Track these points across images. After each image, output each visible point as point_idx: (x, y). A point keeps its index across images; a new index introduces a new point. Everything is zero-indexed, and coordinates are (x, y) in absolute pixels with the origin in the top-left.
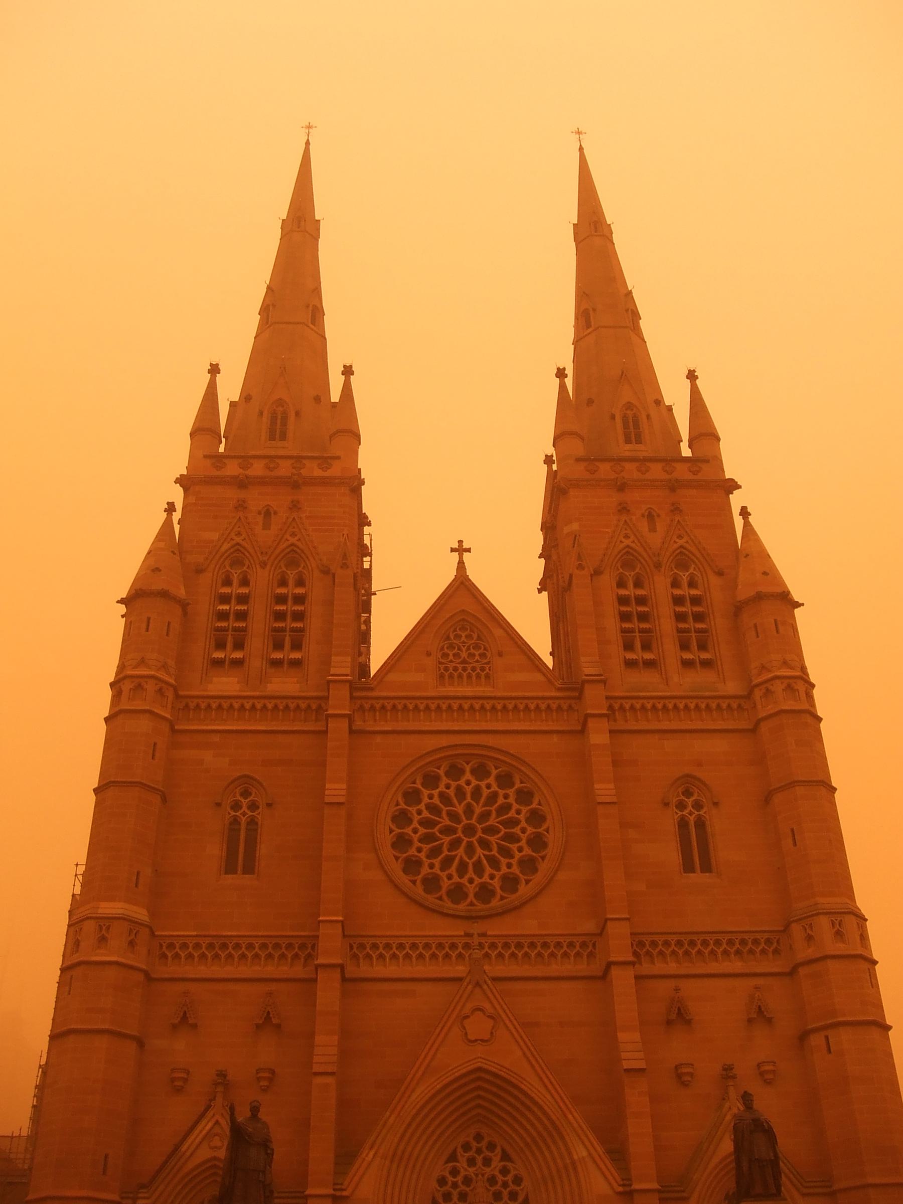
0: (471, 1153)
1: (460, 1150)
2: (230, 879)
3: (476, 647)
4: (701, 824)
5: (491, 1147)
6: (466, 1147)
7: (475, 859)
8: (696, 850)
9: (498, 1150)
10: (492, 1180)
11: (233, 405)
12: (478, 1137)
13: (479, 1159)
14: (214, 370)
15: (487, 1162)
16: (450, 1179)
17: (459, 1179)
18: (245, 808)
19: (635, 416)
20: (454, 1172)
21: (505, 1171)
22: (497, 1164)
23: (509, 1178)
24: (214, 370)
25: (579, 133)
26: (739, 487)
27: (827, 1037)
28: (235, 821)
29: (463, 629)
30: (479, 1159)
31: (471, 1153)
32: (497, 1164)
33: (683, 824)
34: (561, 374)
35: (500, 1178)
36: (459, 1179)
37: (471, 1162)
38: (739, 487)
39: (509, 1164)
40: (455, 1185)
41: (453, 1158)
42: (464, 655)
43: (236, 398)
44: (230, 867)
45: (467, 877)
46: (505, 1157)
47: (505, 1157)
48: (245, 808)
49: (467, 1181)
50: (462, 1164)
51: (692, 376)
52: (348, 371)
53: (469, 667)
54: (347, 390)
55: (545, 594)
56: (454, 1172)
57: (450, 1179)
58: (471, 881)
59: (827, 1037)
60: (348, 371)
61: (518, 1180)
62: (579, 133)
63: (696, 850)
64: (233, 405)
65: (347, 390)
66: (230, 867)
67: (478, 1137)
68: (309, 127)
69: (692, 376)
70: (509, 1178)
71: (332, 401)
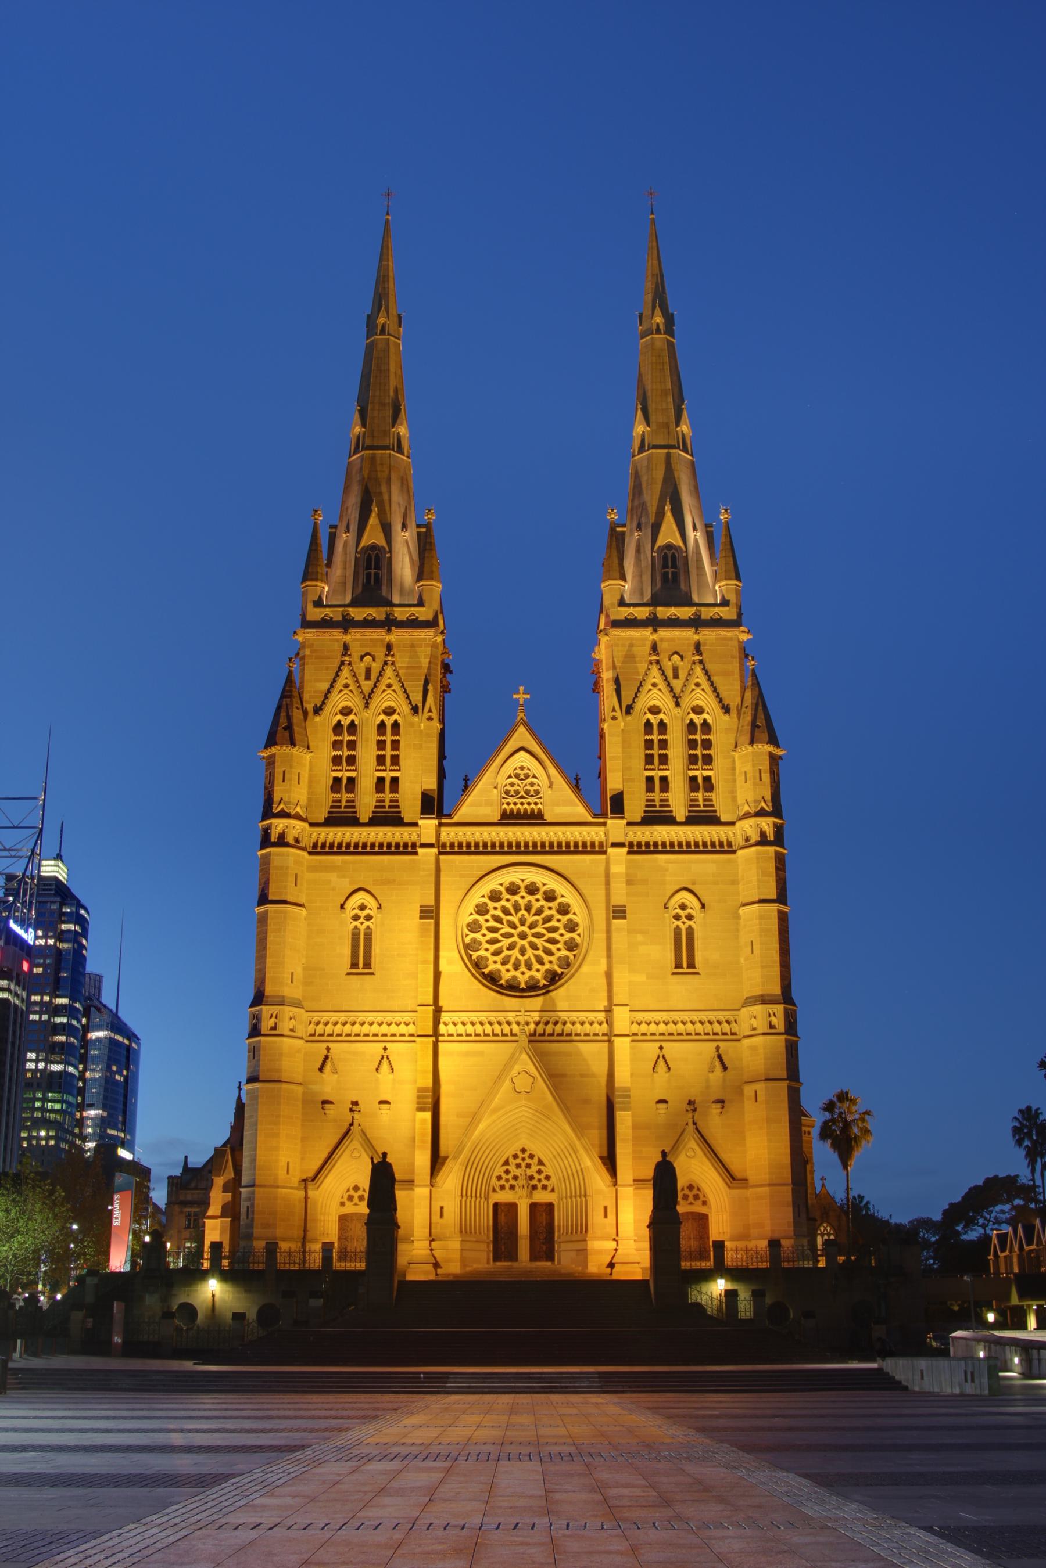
1: (511, 1160)
4: (690, 932)
5: (531, 1156)
6: (515, 1156)
9: (536, 1160)
10: (532, 1178)
12: (523, 1150)
13: (523, 1164)
15: (528, 1166)
16: (504, 1176)
17: (510, 1176)
19: (673, 555)
20: (507, 1172)
21: (539, 1172)
22: (535, 1168)
23: (542, 1176)
30: (523, 1164)
31: (518, 1161)
32: (535, 1168)
33: (677, 932)
35: (536, 1176)
36: (510, 1176)
37: (518, 1166)
39: (542, 1168)
40: (507, 1180)
41: (507, 1163)
47: (540, 1162)
49: (515, 1178)
50: (512, 1168)
56: (507, 1172)
57: (504, 1176)
61: (548, 1178)
67: (523, 1150)
70: (542, 1176)
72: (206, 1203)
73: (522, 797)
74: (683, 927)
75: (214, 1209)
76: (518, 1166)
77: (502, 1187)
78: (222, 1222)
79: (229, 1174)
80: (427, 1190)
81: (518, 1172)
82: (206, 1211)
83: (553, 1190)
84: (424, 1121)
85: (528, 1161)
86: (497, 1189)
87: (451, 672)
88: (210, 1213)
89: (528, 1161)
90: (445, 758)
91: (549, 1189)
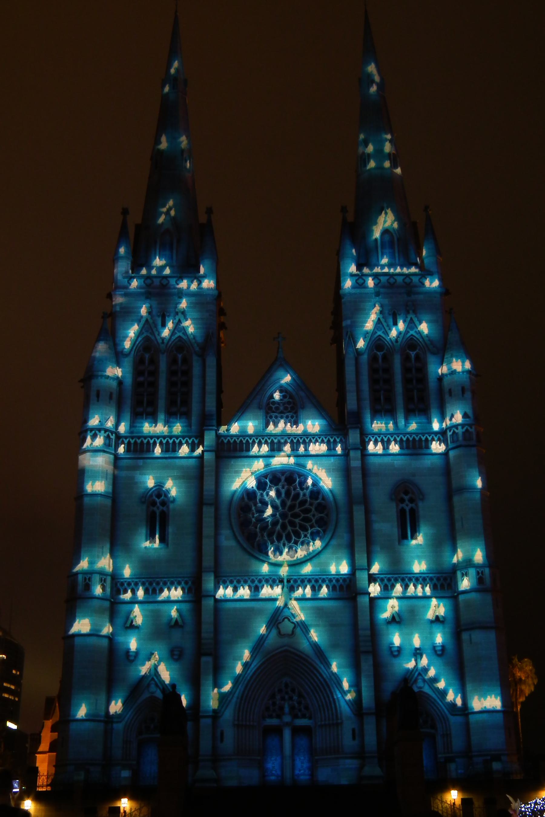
7: (287, 532)
14: (125, 212)
24: (125, 212)
27: (470, 636)
28: (154, 513)
34: (344, 210)
45: (282, 542)
46: (300, 695)
47: (300, 695)
52: (209, 211)
56: (274, 704)
59: (470, 636)
60: (209, 211)
72: (37, 741)
75: (44, 746)
78: (49, 756)
79: (56, 717)
82: (38, 748)
88: (41, 749)
90: (222, 392)
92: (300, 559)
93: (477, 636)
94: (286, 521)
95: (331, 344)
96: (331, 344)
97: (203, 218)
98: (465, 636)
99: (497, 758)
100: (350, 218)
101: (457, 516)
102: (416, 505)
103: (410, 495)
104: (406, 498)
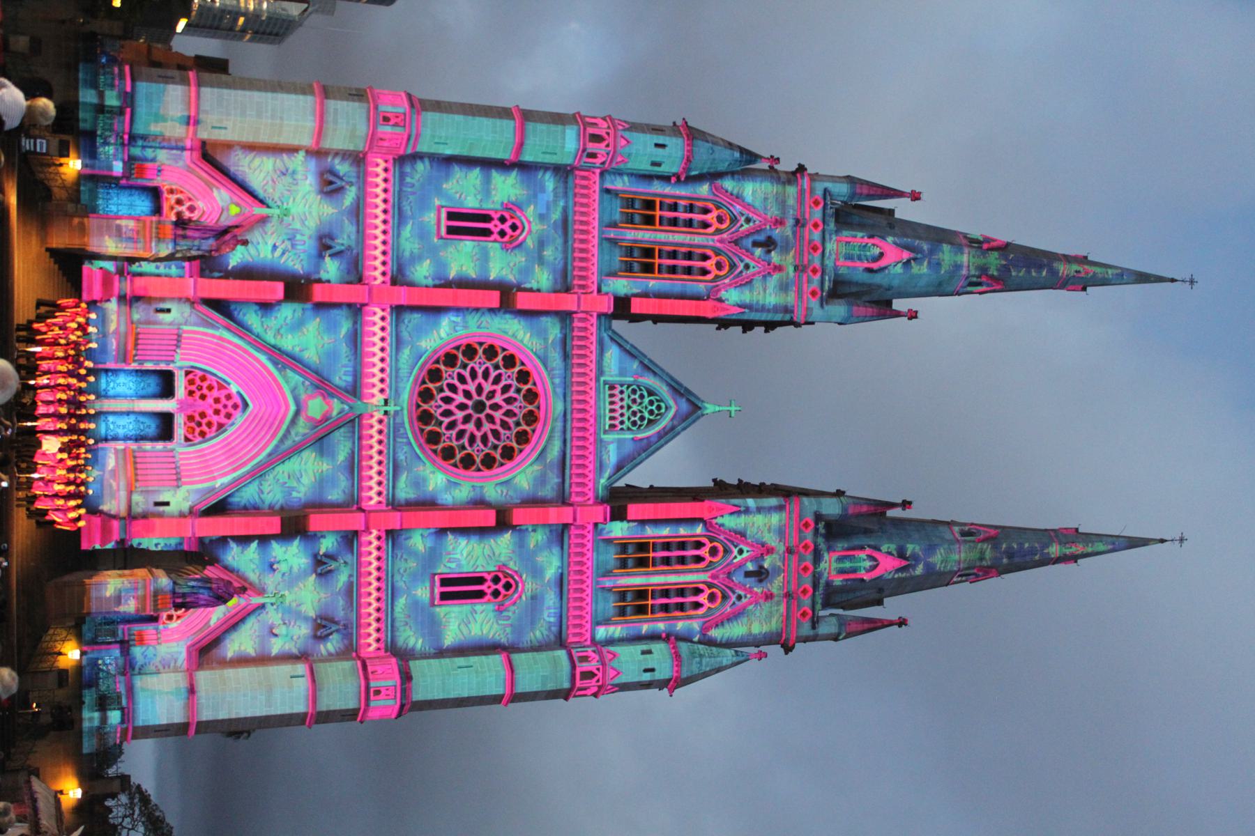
0: (223, 400)
1: (224, 392)
2: (443, 215)
3: (642, 418)
8: (461, 588)
9: (223, 420)
11: (891, 212)
13: (219, 406)
14: (915, 196)
15: (217, 412)
16: (205, 384)
18: (501, 226)
21: (209, 425)
24: (915, 196)
25: (1182, 540)
26: (786, 653)
29: (659, 408)
30: (219, 406)
31: (223, 400)
34: (906, 504)
36: (205, 391)
37: (217, 401)
38: (786, 653)
39: (214, 428)
42: (635, 408)
43: (897, 215)
44: (451, 216)
48: (501, 226)
49: (203, 397)
50: (215, 393)
51: (902, 623)
52: (913, 315)
53: (624, 411)
54: (898, 314)
55: (712, 484)
56: (210, 388)
57: (205, 384)
58: (438, 407)
60: (913, 315)
62: (1182, 540)
63: (461, 588)
64: (891, 212)
65: (898, 314)
66: (451, 216)
68: (1192, 282)
69: (902, 623)
70: (205, 428)
71: (894, 301)
73: (629, 407)
74: (483, 587)
76: (217, 401)
77: (191, 382)
80: (191, 293)
81: (210, 400)
83: (187, 439)
84: (274, 291)
85: (223, 412)
86: (191, 376)
87: (766, 331)
89: (223, 412)
90: (655, 322)
91: (190, 436)
92: (755, 636)
93: (302, 685)
94: (470, 411)
95: (714, 480)
96: (714, 480)
97: (899, 304)
98: (301, 668)
99: (127, 715)
100: (891, 513)
101: (473, 660)
102: (489, 601)
103: (503, 591)
104: (500, 587)
